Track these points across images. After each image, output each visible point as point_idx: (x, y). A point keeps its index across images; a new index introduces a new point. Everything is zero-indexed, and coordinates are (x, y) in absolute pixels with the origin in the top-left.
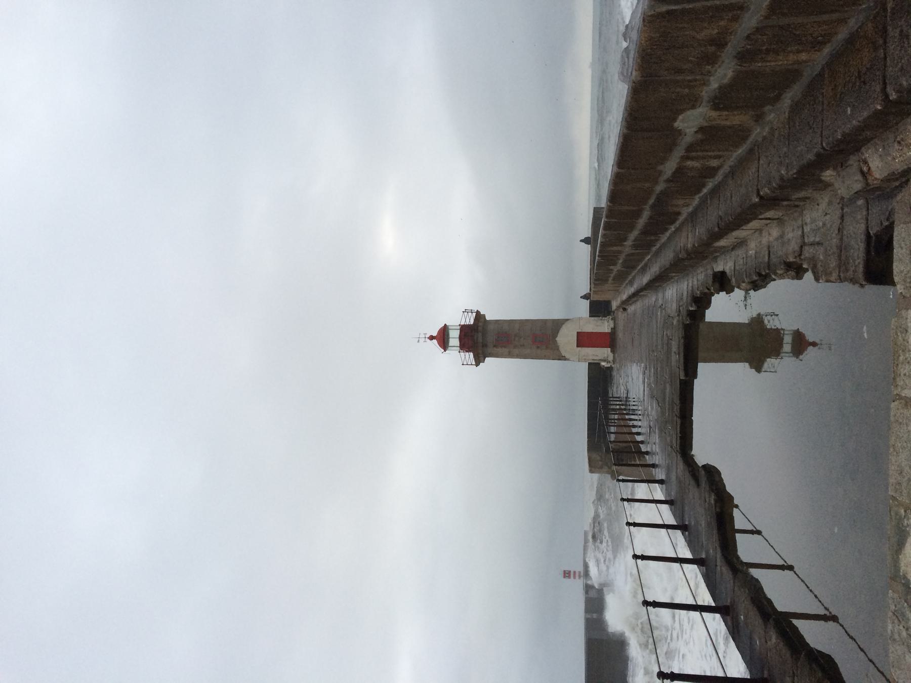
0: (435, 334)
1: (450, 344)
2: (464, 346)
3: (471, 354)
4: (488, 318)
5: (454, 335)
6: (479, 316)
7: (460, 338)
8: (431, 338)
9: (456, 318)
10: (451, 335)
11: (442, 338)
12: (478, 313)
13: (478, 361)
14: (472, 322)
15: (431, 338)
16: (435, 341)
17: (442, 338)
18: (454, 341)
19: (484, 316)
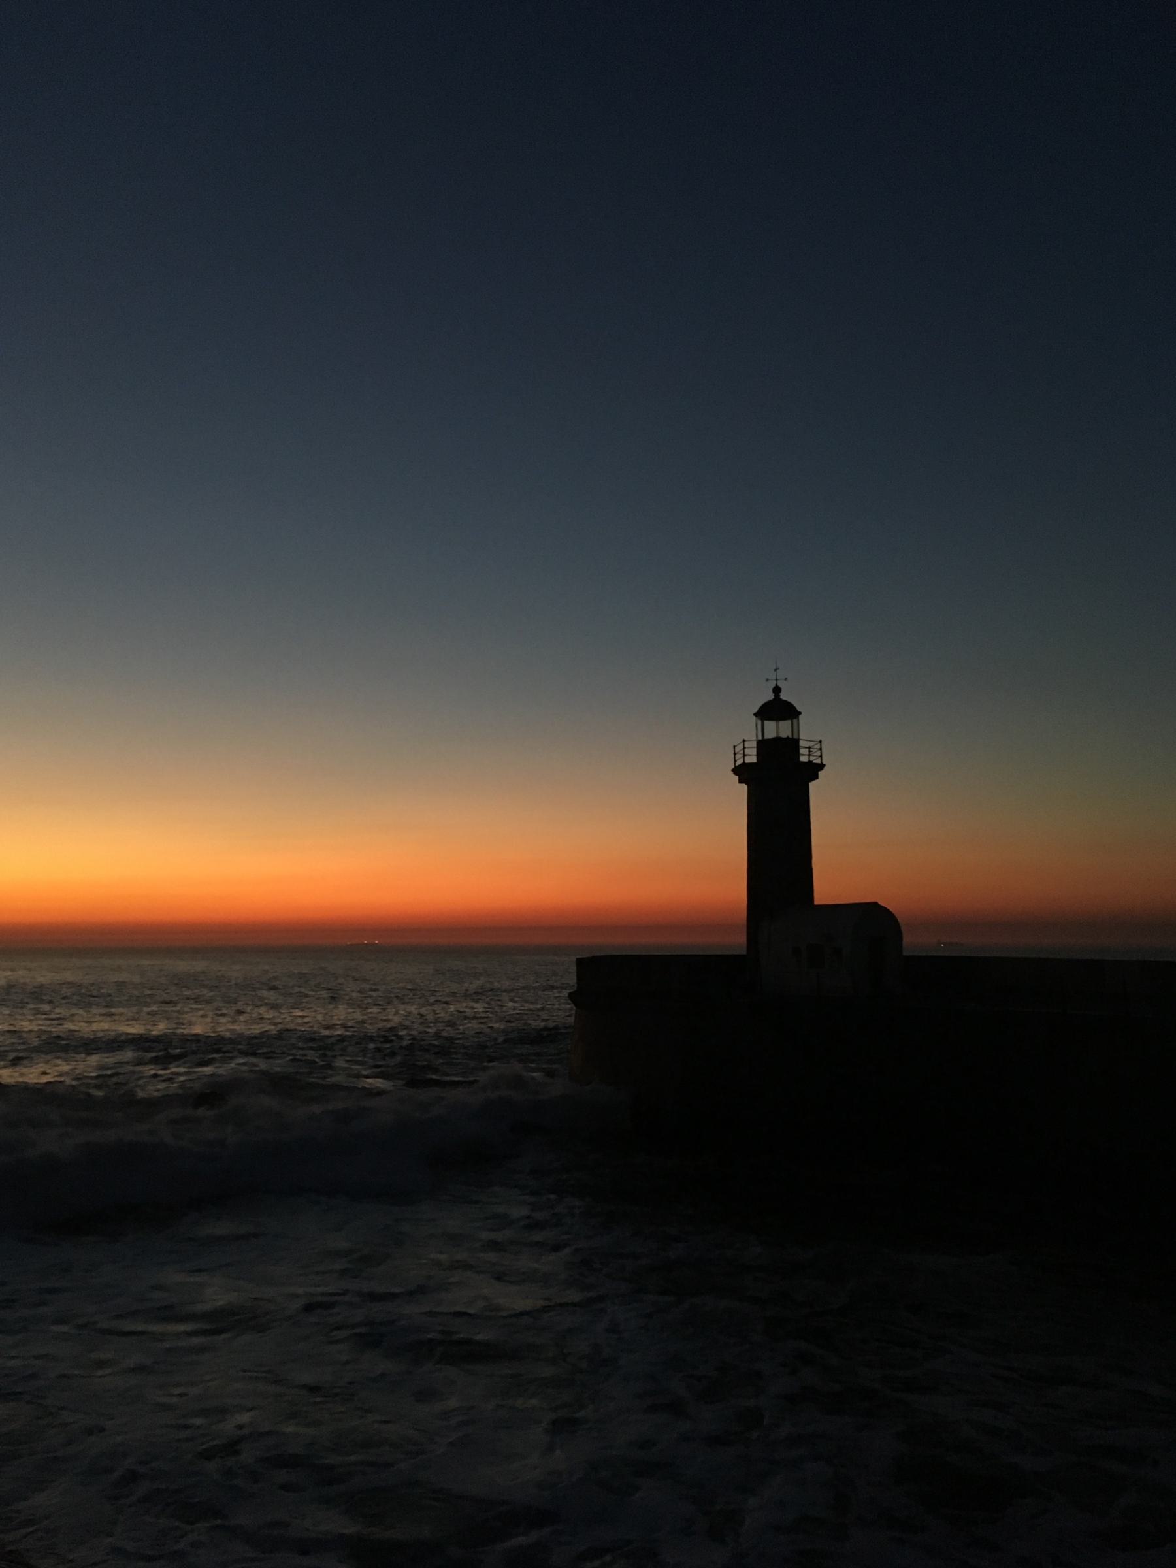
1: (766, 722)
2: (763, 745)
3: (752, 759)
4: (812, 785)
5: (783, 729)
6: (813, 770)
7: (777, 740)
8: (777, 690)
9: (810, 731)
10: (781, 723)
11: (777, 708)
12: (821, 766)
14: (804, 759)
15: (777, 690)
16: (771, 696)
17: (777, 708)
18: (772, 729)
19: (816, 777)
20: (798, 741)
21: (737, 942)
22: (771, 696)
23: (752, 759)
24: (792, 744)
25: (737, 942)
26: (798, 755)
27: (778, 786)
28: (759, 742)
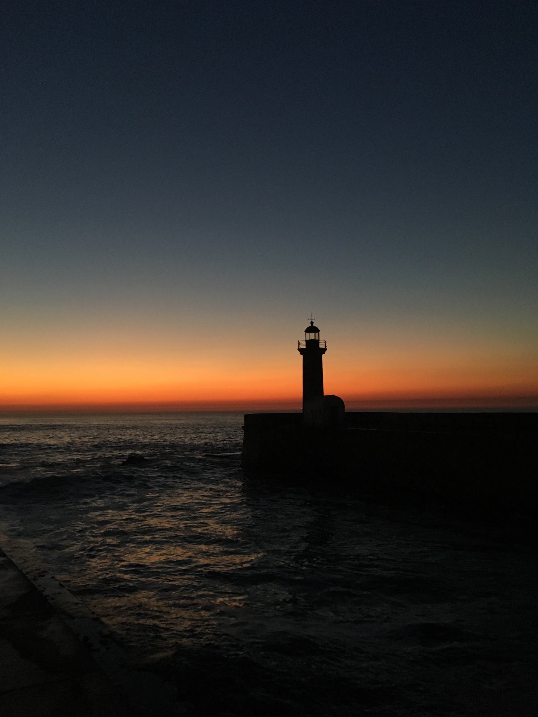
0: (314, 325)
3: (303, 346)
6: (325, 349)
8: (312, 323)
11: (312, 329)
13: (301, 351)
14: (320, 346)
15: (312, 323)
17: (312, 329)
20: (319, 340)
21: (299, 408)
22: (310, 325)
23: (305, 347)
24: (317, 342)
25: (299, 408)
26: (319, 345)
27: (313, 355)
28: (306, 341)
